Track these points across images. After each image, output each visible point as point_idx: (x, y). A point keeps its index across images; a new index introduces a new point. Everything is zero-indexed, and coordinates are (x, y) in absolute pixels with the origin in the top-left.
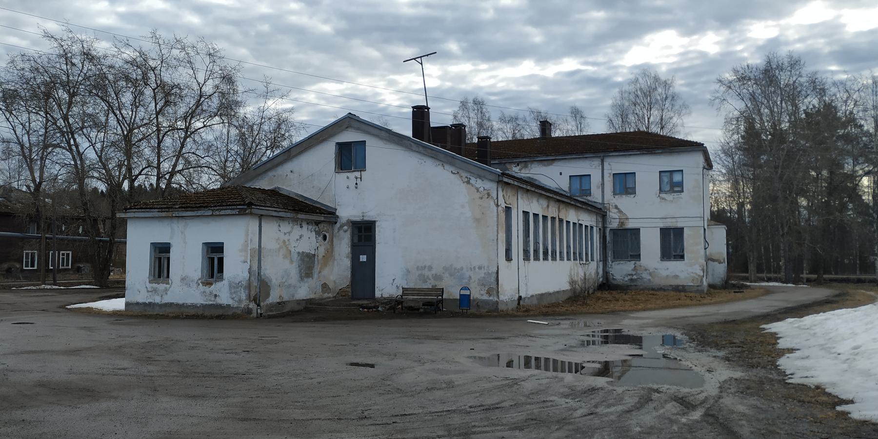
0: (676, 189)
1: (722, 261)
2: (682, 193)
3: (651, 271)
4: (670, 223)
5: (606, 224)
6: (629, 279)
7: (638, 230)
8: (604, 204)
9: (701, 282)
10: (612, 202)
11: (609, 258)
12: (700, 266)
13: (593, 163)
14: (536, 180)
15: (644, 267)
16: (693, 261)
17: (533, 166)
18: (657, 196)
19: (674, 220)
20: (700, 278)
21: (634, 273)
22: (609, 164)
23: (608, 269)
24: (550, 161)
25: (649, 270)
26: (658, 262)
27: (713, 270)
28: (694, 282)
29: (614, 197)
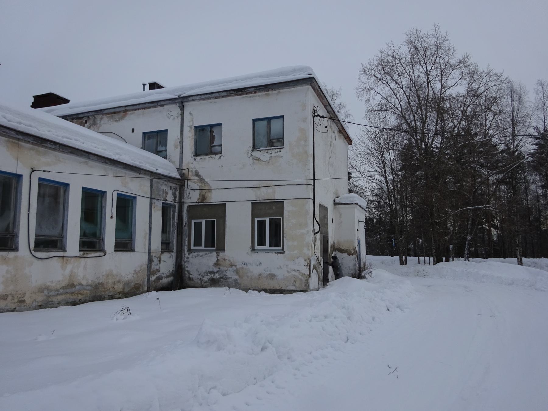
1: (353, 252)
2: (282, 150)
3: (238, 267)
4: (265, 195)
5: (184, 199)
6: (209, 279)
7: (223, 206)
8: (182, 169)
9: (306, 285)
10: (191, 166)
11: (186, 248)
12: (305, 260)
13: (171, 114)
15: (229, 261)
17: (102, 122)
19: (270, 190)
20: (304, 279)
21: (216, 270)
22: (190, 114)
23: (183, 263)
25: (236, 266)
26: (248, 253)
29: (195, 159)
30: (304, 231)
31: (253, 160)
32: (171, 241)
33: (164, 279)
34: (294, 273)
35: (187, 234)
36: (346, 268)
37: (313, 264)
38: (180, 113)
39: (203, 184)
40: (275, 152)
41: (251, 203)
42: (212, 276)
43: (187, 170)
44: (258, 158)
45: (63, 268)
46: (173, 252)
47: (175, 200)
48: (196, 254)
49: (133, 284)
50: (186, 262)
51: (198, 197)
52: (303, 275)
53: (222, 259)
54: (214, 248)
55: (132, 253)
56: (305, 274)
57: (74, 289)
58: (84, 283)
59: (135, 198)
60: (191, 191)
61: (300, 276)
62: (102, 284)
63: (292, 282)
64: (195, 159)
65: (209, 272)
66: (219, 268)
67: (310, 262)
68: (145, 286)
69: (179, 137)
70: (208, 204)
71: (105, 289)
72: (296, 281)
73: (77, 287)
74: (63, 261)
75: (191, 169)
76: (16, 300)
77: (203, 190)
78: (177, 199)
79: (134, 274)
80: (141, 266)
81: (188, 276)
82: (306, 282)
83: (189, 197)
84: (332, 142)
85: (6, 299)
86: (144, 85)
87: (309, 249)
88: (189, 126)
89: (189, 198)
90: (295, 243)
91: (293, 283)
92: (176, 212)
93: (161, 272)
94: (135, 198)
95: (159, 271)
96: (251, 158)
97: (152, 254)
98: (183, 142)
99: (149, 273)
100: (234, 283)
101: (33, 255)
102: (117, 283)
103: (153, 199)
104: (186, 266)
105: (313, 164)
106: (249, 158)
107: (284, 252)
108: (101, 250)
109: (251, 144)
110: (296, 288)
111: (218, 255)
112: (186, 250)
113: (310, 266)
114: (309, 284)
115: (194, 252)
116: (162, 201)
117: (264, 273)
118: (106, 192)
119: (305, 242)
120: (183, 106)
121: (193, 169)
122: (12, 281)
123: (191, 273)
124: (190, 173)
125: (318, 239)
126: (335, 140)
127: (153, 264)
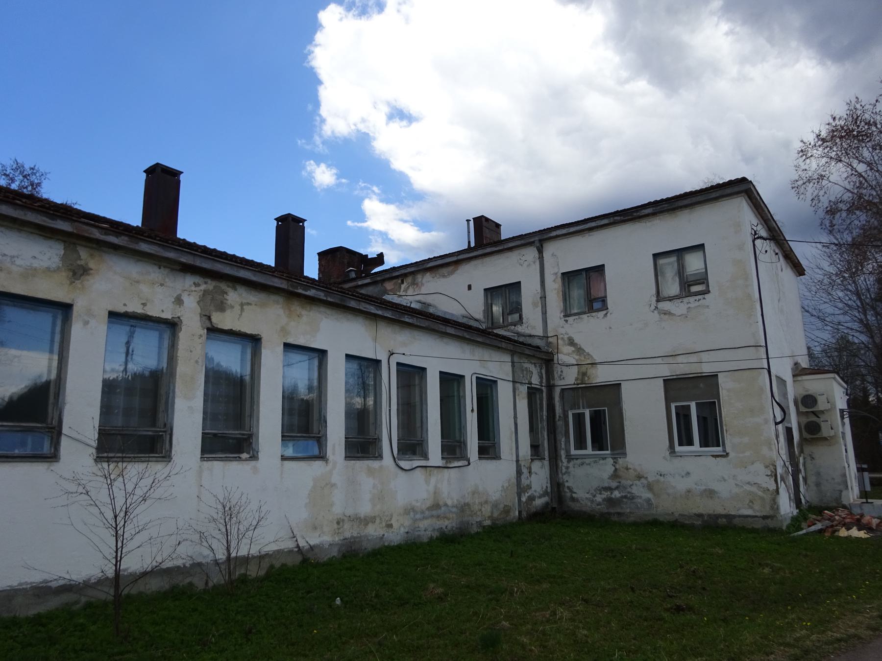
0: (694, 289)
2: (706, 296)
3: (650, 479)
4: (684, 367)
5: (554, 379)
6: (604, 500)
7: (617, 386)
8: (548, 337)
9: (772, 508)
10: (562, 331)
11: (563, 453)
12: (766, 467)
13: (524, 258)
14: (429, 305)
15: (635, 470)
16: (747, 454)
17: (425, 280)
18: (653, 307)
19: (693, 358)
20: (768, 497)
21: (614, 484)
22: (553, 255)
23: (560, 475)
24: (451, 268)
25: (647, 478)
26: (664, 458)
27: (818, 474)
28: (757, 507)
29: (566, 321)
31: (660, 315)
32: (540, 443)
33: (537, 499)
35: (563, 432)
38: (537, 256)
39: (582, 356)
40: (696, 300)
41: (662, 382)
42: (608, 495)
43: (556, 337)
44: (667, 311)
45: (427, 482)
46: (544, 459)
47: (541, 382)
48: (579, 461)
49: (502, 506)
50: (564, 474)
51: (576, 376)
53: (623, 468)
54: (608, 452)
55: (498, 462)
56: (768, 490)
57: (439, 512)
58: (449, 503)
59: (497, 381)
60: (564, 369)
61: (760, 492)
62: (468, 505)
64: (566, 321)
65: (603, 488)
66: (620, 482)
68: (516, 509)
69: (539, 290)
70: (592, 385)
71: (472, 511)
73: (443, 509)
74: (426, 472)
75: (562, 336)
76: (384, 524)
77: (583, 366)
78: (544, 381)
79: (502, 491)
80: (509, 480)
81: (570, 495)
82: (772, 502)
83: (562, 377)
85: (375, 522)
86: (468, 221)
87: (770, 449)
88: (552, 273)
89: (561, 378)
90: (746, 440)
91: (748, 505)
92: (544, 400)
93: (533, 489)
94: (495, 382)
95: (531, 488)
96: (656, 312)
97: (520, 462)
98: (545, 297)
99: (519, 490)
100: (645, 505)
101: (397, 465)
102: (484, 504)
103: (516, 382)
104: (565, 480)
106: (653, 312)
107: (727, 454)
108: (464, 457)
109: (654, 291)
110: (755, 512)
111: (615, 462)
112: (563, 456)
113: (776, 476)
115: (577, 459)
116: (527, 385)
117: (696, 488)
118: (464, 376)
120: (542, 246)
121: (564, 335)
122: (379, 499)
123: (575, 490)
124: (559, 341)
126: (782, 270)
127: (523, 477)
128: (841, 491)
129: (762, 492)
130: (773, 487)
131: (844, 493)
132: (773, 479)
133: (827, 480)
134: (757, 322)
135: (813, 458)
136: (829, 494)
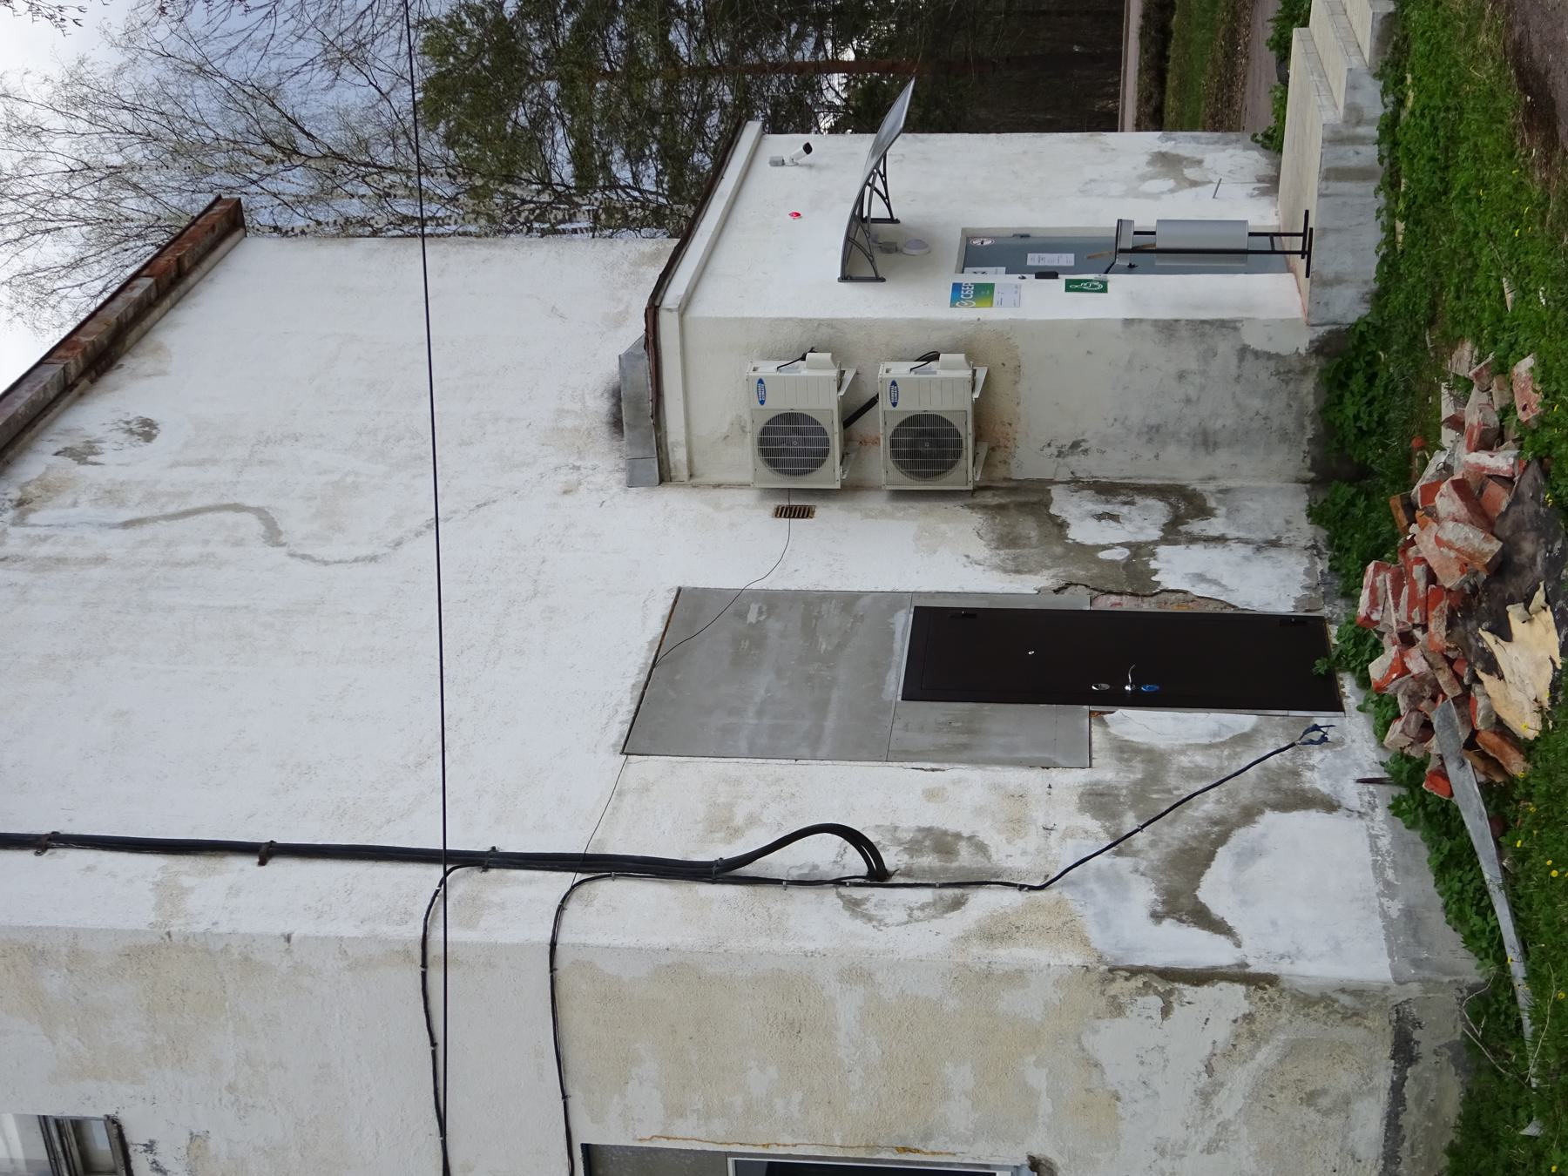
2: (136, 1136)
12: (1117, 1008)
20: (1289, 1027)
27: (1154, 433)
30: (847, 1006)
34: (1230, 1102)
36: (1188, 401)
37: (1157, 917)
52: (1252, 1035)
56: (1249, 1018)
61: (1260, 1056)
63: (1312, 1115)
67: (1134, 972)
72: (1309, 1088)
82: (1321, 1009)
84: (151, 497)
90: (960, 1076)
91: (1327, 1113)
105: (249, 863)
113: (1170, 975)
114: (1343, 991)
119: (952, 1004)
125: (931, 795)
128: (1244, 351)
129: (1258, 1046)
130: (1234, 998)
131: (1257, 342)
132: (1188, 991)
133: (1188, 401)
134: (288, 939)
135: (1075, 445)
136: (1256, 403)
